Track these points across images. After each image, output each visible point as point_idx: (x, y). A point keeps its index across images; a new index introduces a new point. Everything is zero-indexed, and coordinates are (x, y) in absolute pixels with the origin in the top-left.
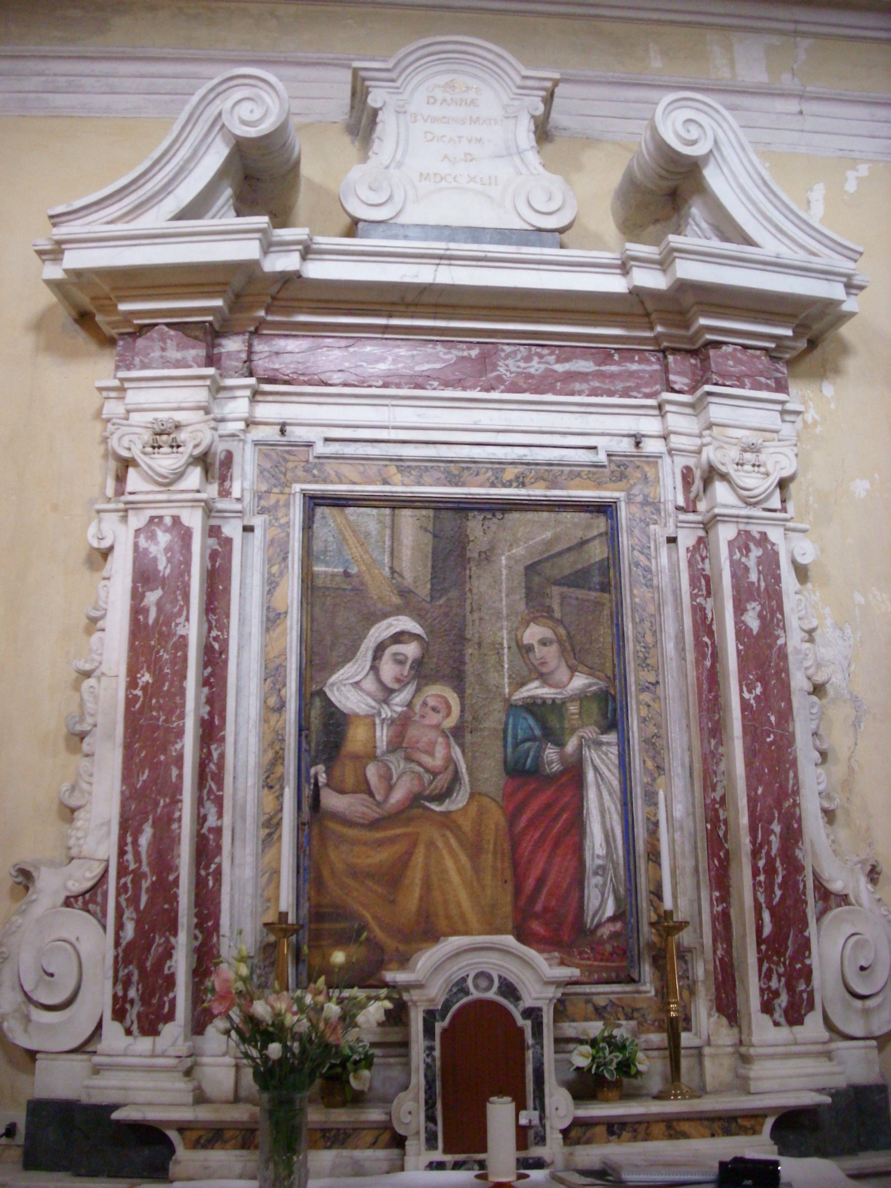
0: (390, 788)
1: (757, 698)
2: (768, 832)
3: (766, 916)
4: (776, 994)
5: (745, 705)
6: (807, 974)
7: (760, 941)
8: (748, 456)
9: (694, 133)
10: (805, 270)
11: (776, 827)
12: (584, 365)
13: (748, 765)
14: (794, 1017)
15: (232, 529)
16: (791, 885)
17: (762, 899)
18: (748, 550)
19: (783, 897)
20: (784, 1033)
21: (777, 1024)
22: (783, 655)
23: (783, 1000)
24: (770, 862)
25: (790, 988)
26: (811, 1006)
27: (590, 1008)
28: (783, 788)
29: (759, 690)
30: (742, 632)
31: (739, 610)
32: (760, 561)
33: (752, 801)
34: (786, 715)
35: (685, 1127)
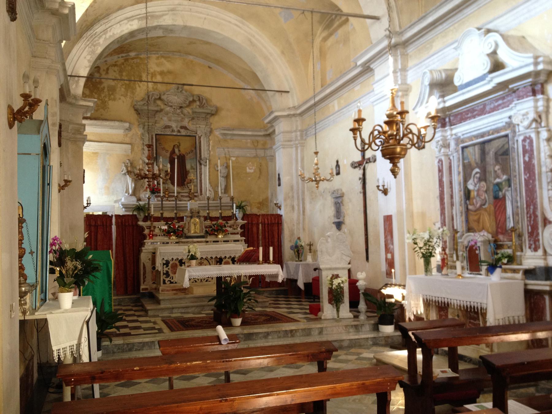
0: (477, 204)
1: (528, 177)
2: (530, 208)
3: (530, 228)
4: (531, 245)
5: (525, 179)
6: (538, 240)
7: (528, 233)
8: (525, 117)
9: (490, 46)
10: (521, 67)
11: (532, 207)
12: (500, 102)
13: (526, 193)
14: (536, 250)
15: (451, 158)
16: (535, 220)
17: (529, 224)
18: (526, 141)
19: (533, 223)
20: (533, 253)
21: (532, 251)
22: (534, 165)
23: (533, 246)
24: (530, 215)
25: (535, 243)
26: (539, 248)
27: (507, 247)
28: (533, 197)
29: (528, 175)
30: (525, 162)
31: (524, 156)
32: (529, 143)
33: (527, 201)
34: (534, 181)
35: (508, 271)
